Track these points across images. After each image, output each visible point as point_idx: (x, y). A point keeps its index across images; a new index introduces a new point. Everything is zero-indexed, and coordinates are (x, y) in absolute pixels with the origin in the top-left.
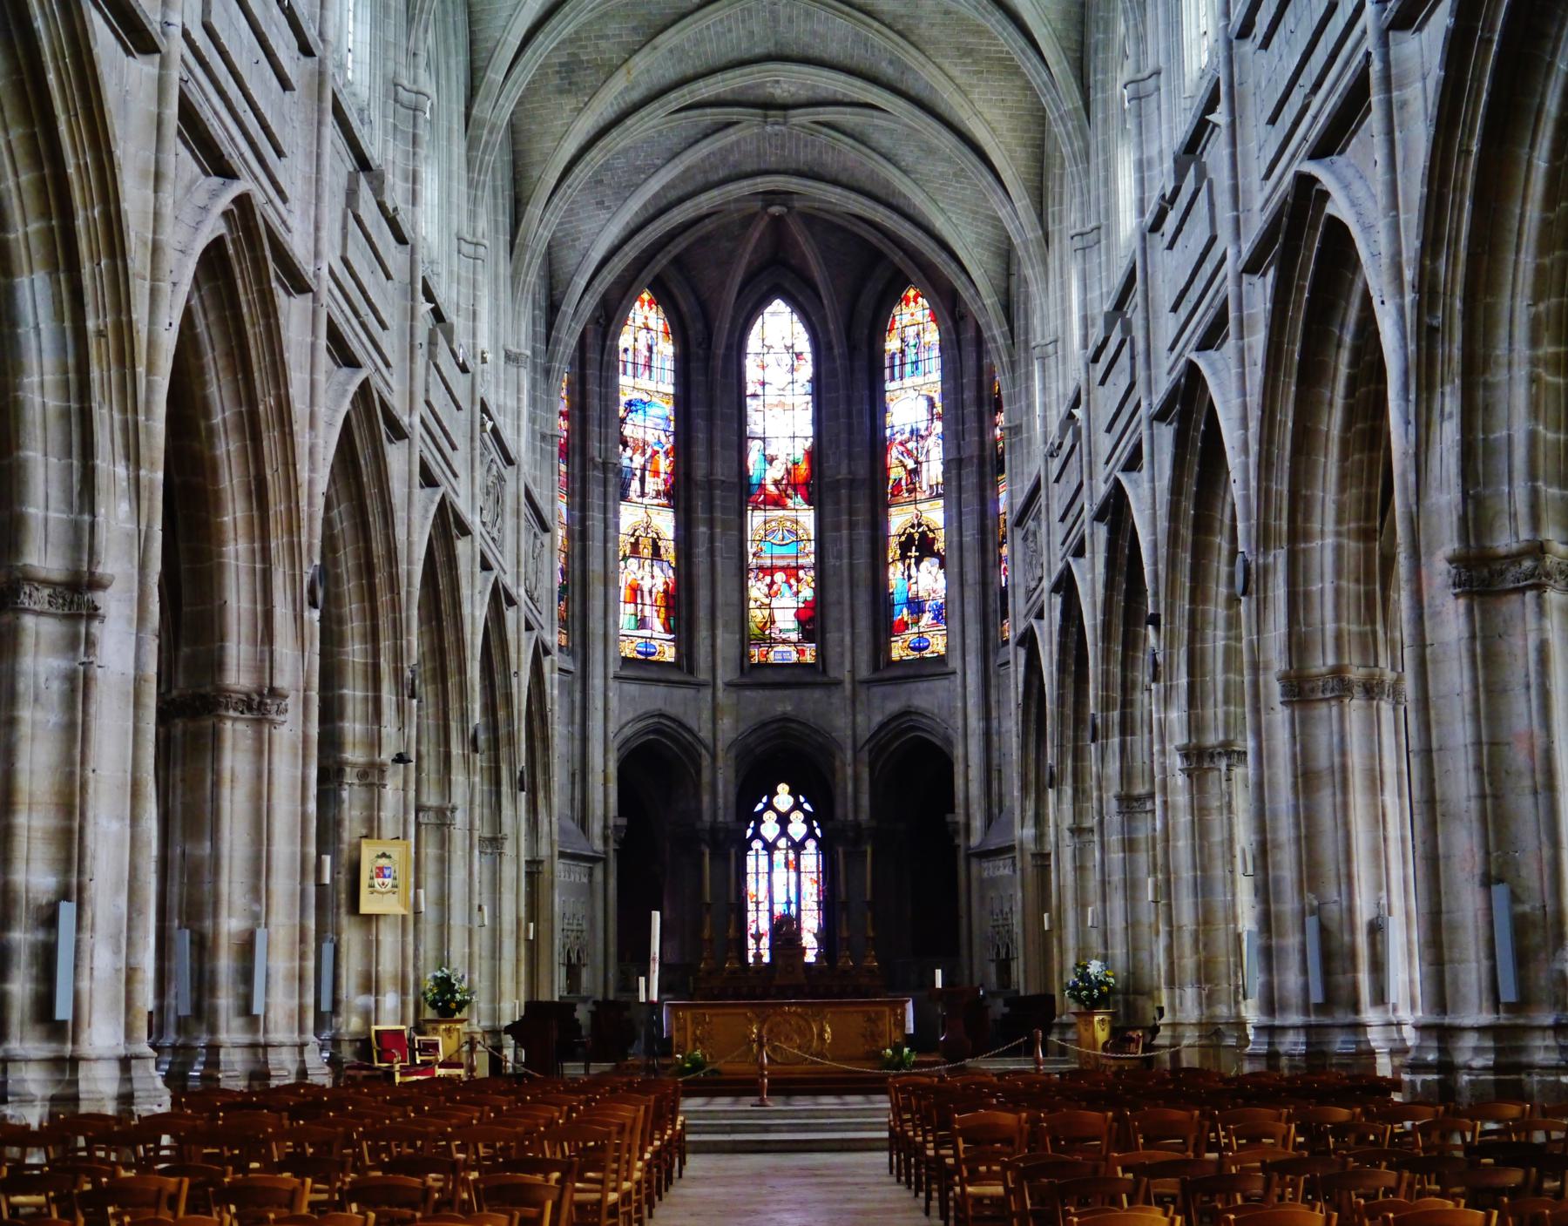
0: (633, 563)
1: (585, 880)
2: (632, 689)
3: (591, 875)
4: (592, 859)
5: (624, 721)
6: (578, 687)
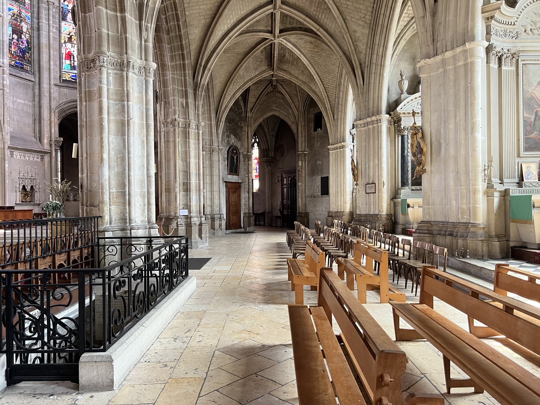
0: (69, 45)
1: (39, 160)
2: (65, 90)
3: (42, 159)
4: (42, 153)
5: (61, 102)
6: (37, 87)
